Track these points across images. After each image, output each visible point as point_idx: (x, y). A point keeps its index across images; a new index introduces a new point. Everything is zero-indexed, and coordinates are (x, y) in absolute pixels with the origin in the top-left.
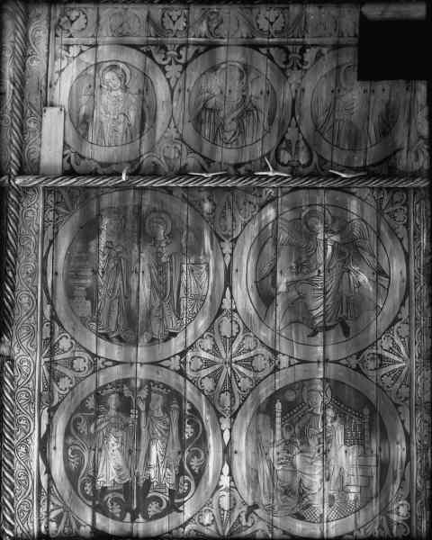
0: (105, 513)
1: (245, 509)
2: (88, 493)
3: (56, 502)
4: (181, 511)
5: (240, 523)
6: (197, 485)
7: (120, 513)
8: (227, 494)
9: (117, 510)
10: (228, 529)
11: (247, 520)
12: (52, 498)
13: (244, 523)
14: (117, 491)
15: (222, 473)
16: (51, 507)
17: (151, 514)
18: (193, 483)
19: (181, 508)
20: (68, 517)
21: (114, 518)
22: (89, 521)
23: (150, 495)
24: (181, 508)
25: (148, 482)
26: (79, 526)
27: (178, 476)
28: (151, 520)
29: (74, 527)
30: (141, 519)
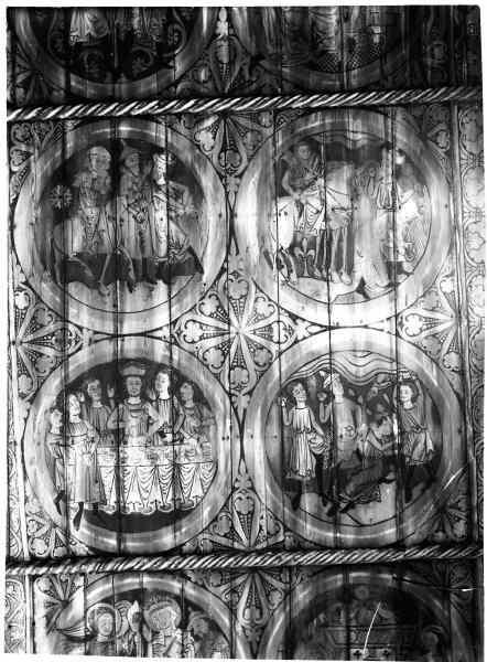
0: (81, 73)
1: (248, 60)
2: (59, 50)
3: (22, 64)
4: (171, 67)
5: (243, 77)
6: (188, 39)
7: (99, 73)
8: (225, 44)
9: (95, 71)
10: (228, 87)
11: (250, 74)
12: (18, 59)
13: (247, 77)
14: (96, 47)
15: (218, 19)
16: (17, 70)
17: (136, 72)
18: (184, 35)
19: (171, 64)
20: (37, 81)
21: (92, 79)
22: (62, 83)
23: (133, 49)
24: (171, 64)
25: (131, 33)
26: (51, 90)
27: (165, 26)
28: (135, 80)
29: (46, 92)
30: (124, 79)
